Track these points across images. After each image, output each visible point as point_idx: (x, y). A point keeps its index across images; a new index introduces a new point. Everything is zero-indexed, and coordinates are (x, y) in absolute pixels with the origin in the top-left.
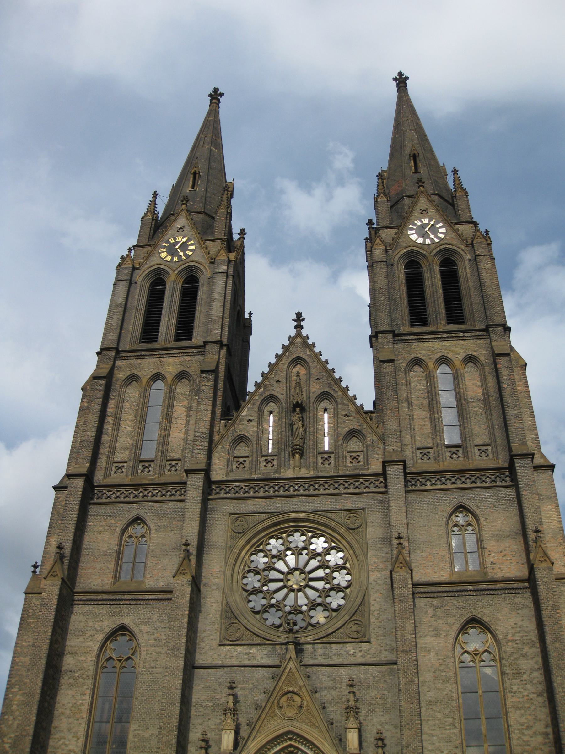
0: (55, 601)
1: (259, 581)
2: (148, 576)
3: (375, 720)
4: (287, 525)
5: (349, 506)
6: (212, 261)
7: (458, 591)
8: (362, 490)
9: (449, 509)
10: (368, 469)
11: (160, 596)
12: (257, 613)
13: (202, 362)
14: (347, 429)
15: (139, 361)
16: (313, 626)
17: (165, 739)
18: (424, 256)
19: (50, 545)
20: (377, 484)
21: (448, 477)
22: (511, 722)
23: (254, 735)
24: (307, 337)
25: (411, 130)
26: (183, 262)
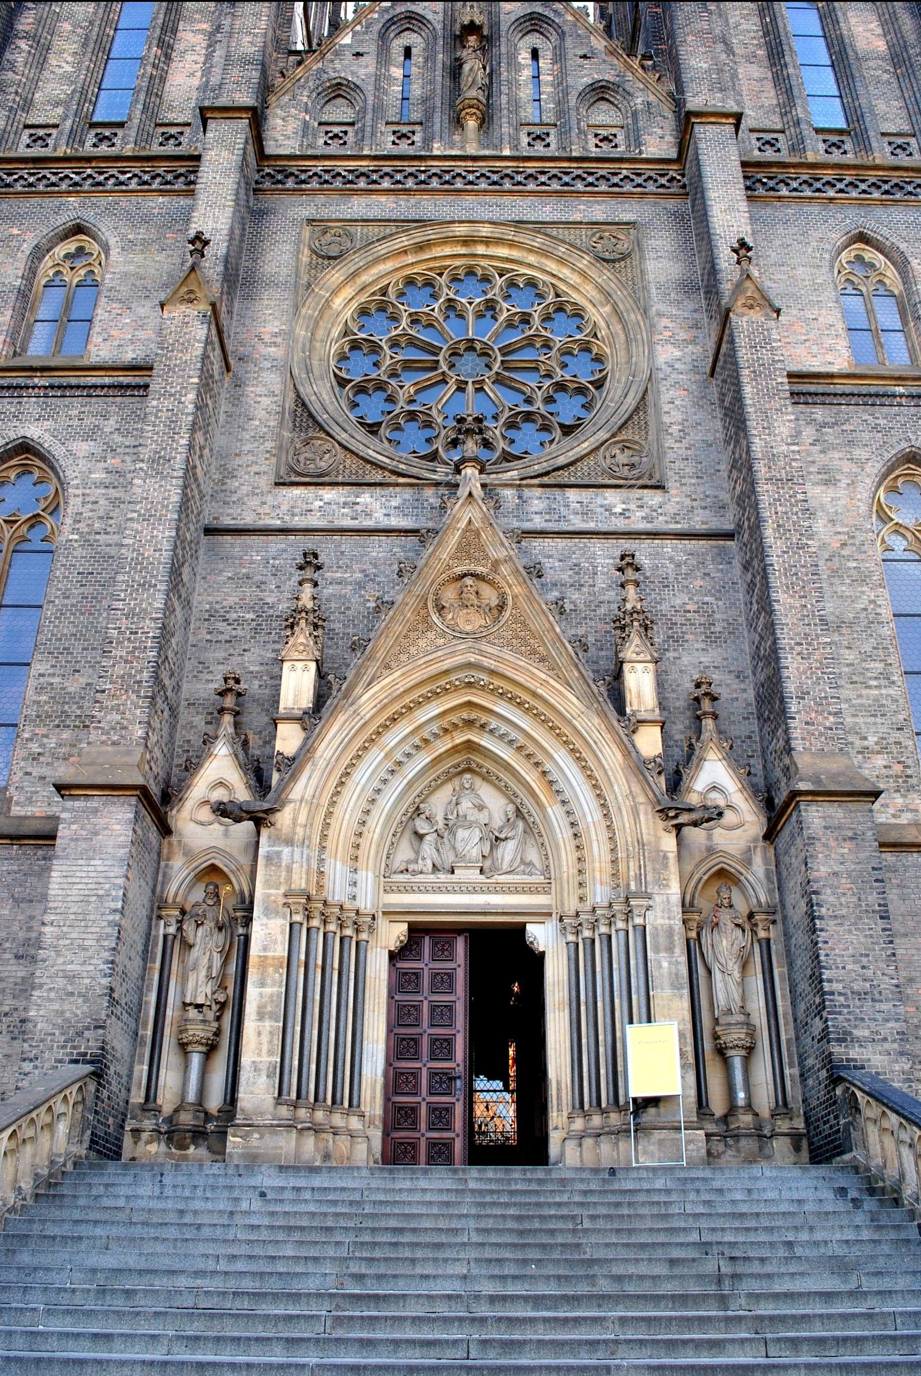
3: (685, 660)
4: (448, 251)
5: (601, 218)
8: (628, 187)
9: (837, 237)
14: (587, 80)
17: (119, 670)
23: (371, 671)
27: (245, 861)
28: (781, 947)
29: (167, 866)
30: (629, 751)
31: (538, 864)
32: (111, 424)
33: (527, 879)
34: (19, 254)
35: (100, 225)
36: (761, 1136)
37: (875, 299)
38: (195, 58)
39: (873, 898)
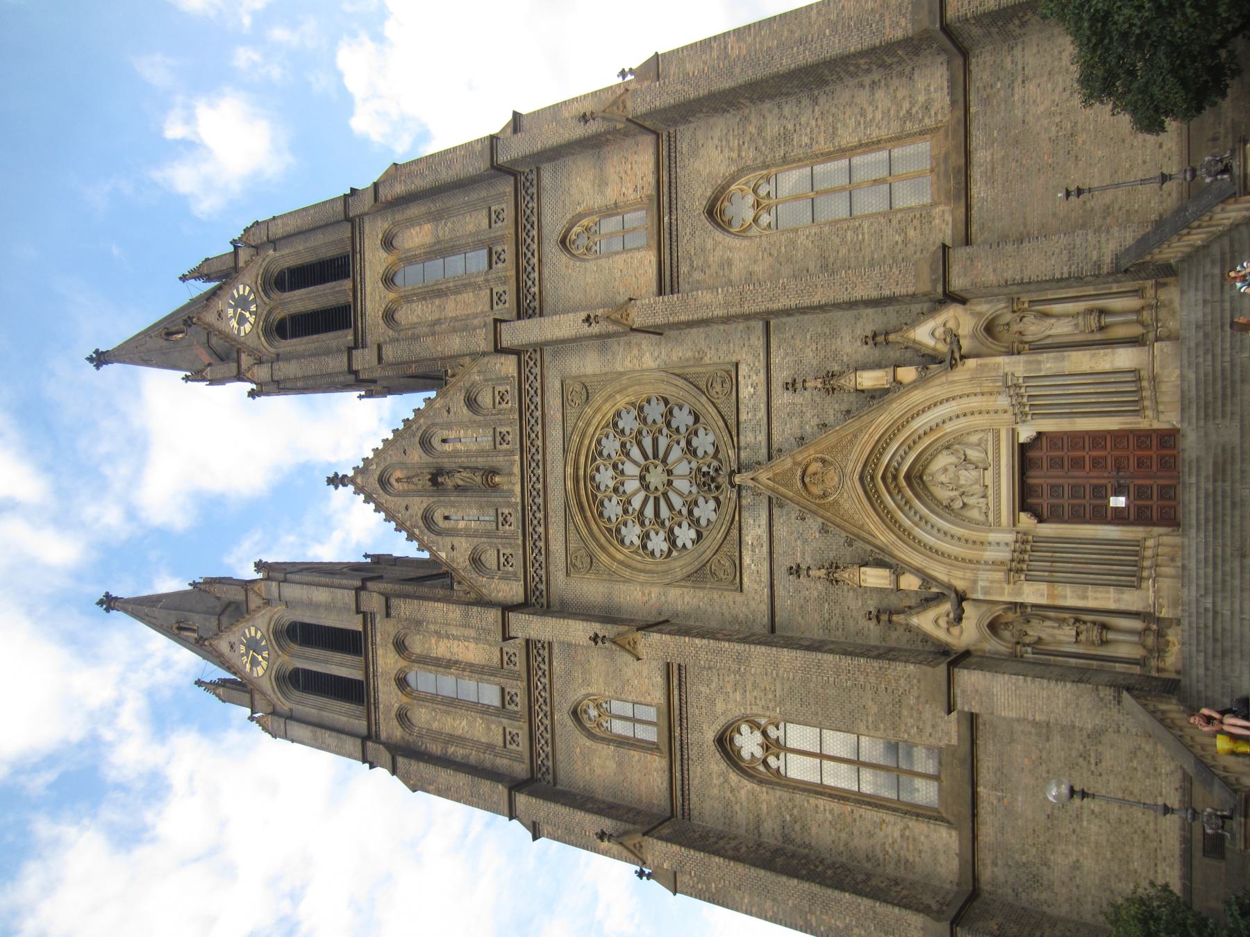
0: (675, 848)
1: (657, 534)
2: (649, 699)
3: (848, 350)
4: (583, 492)
5: (559, 401)
6: (268, 602)
8: (538, 384)
9: (564, 258)
10: (513, 377)
12: (699, 535)
14: (465, 410)
15: (381, 706)
16: (717, 451)
17: (872, 679)
18: (270, 312)
20: (531, 363)
22: (854, 141)
23: (866, 536)
24: (356, 469)
27: (984, 608)
28: (1034, 294)
29: (989, 652)
30: (914, 385)
31: (980, 435)
34: (594, 747)
35: (573, 699)
37: (602, 232)
38: (455, 646)
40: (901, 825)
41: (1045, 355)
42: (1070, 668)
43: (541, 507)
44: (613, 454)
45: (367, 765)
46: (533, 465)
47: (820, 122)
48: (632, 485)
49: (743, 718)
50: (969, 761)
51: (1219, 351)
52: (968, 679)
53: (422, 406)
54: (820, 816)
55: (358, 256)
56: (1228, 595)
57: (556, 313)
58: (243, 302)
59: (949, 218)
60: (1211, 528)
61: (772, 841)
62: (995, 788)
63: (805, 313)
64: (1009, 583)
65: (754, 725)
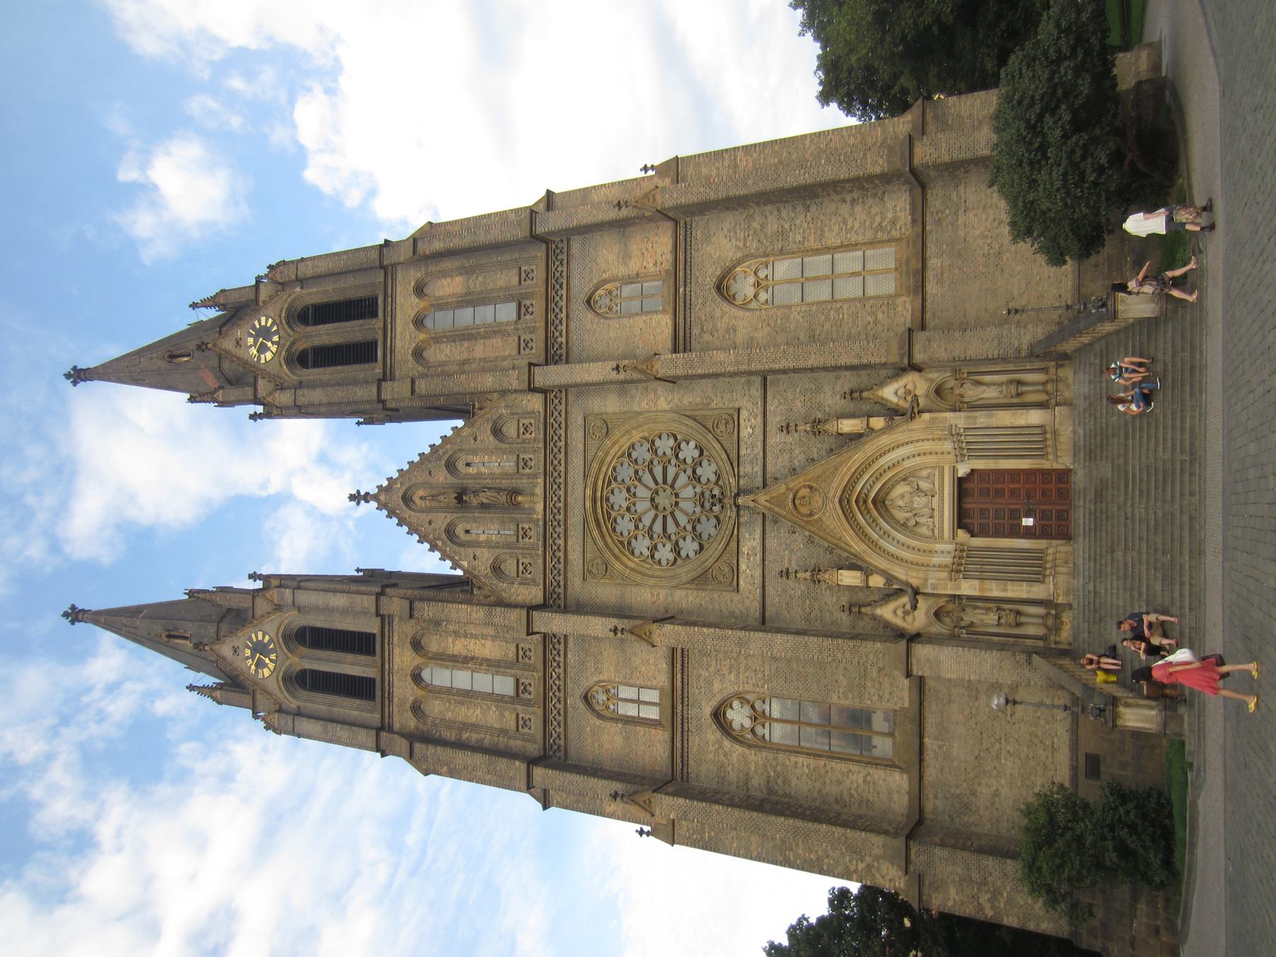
0: (681, 801)
1: (664, 546)
2: (655, 682)
3: (830, 402)
4: (599, 510)
5: (581, 434)
6: (279, 608)
7: (685, 305)
8: (562, 419)
9: (590, 315)
10: (539, 412)
11: (679, 667)
13: (400, 617)
14: (491, 438)
15: (395, 700)
16: (718, 479)
17: (848, 655)
18: (293, 343)
19: (615, 812)
20: (556, 401)
21: (553, 317)
23: (843, 545)
24: (380, 487)
25: (140, 363)
26: (277, 646)
27: (932, 600)
30: (883, 431)
31: (929, 471)
32: (704, 673)
33: (937, 476)
35: (585, 686)
36: (1057, 381)
38: (472, 644)
39: (957, 334)
40: (864, 773)
41: (979, 413)
42: (994, 643)
43: (562, 523)
44: (627, 480)
45: (379, 754)
46: (555, 487)
47: (810, 224)
48: (642, 506)
49: (736, 694)
50: (918, 719)
51: (1098, 415)
52: (922, 651)
53: (449, 433)
54: (798, 771)
55: (390, 299)
56: (1104, 579)
57: (580, 362)
58: (265, 333)
59: (909, 306)
60: (1093, 535)
61: (759, 795)
62: (936, 739)
63: (798, 373)
64: (951, 580)
65: (744, 701)
